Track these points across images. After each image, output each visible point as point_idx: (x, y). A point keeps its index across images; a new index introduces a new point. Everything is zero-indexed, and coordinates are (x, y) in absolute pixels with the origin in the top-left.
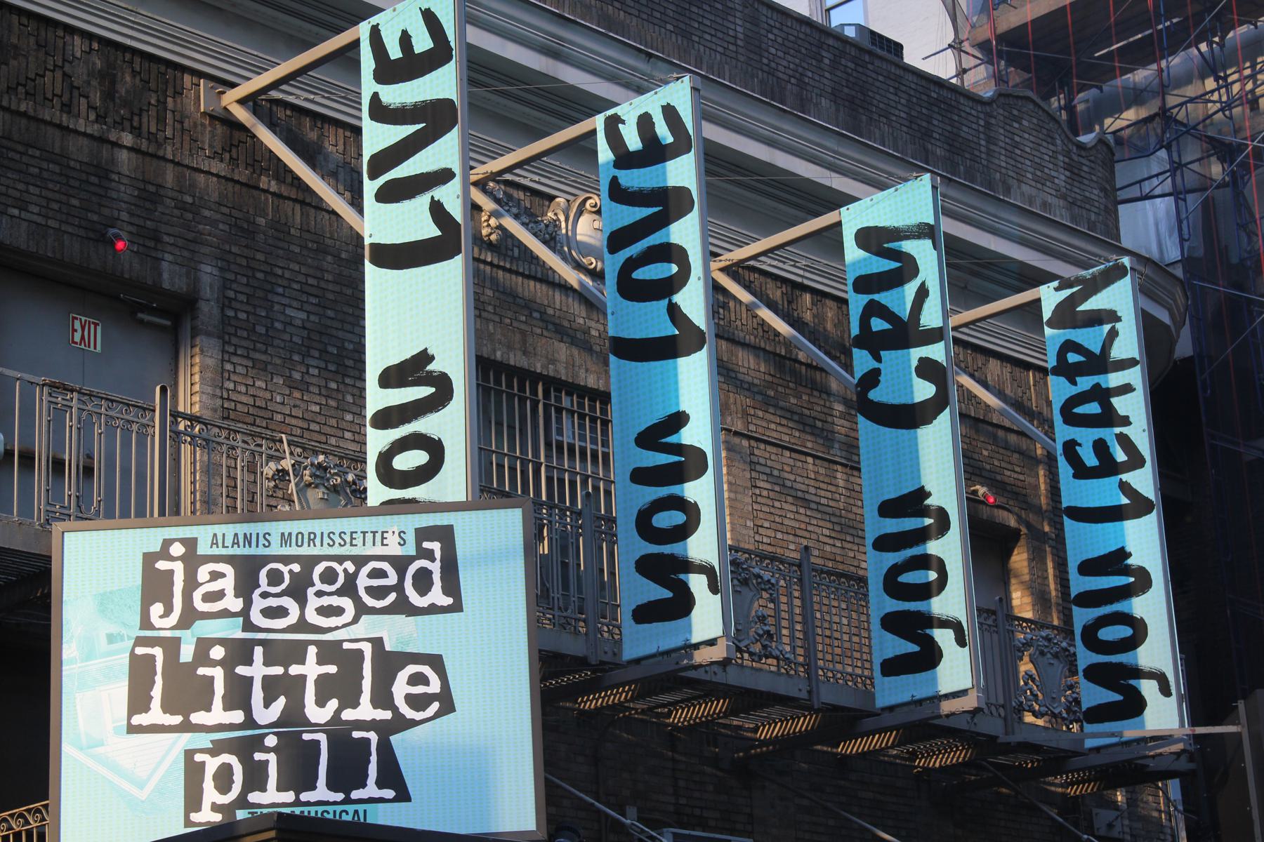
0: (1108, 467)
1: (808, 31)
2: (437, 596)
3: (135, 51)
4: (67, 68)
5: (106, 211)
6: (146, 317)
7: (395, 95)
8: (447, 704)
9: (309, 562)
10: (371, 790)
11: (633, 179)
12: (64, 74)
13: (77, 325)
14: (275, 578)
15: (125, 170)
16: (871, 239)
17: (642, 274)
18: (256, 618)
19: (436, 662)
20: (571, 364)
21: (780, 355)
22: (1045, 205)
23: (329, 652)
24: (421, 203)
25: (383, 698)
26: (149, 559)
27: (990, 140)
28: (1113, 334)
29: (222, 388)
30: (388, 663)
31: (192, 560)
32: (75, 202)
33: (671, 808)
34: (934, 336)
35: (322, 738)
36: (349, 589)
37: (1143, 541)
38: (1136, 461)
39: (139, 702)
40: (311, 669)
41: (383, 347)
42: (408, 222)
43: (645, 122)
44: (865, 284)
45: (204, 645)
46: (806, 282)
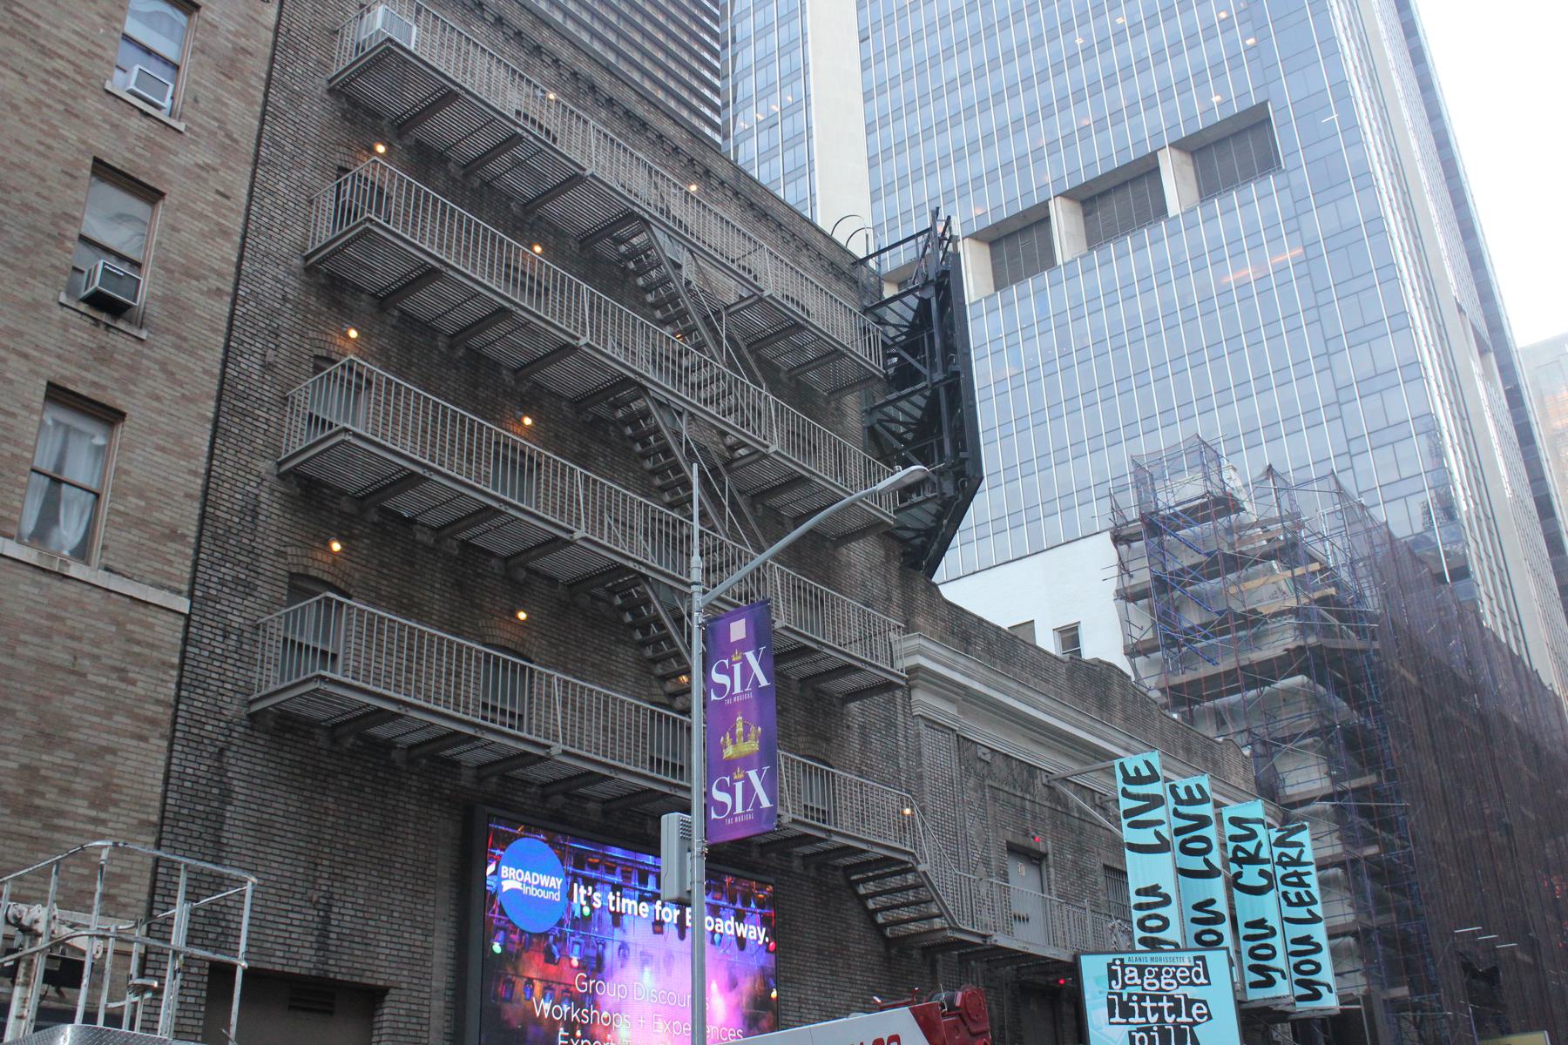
0: (1301, 903)
2: (1202, 980)
7: (1132, 789)
8: (1210, 1018)
9: (1160, 967)
11: (1183, 809)
14: (1150, 973)
16: (1236, 821)
17: (1190, 845)
19: (1205, 1002)
23: (1170, 998)
24: (1151, 830)
25: (1189, 1015)
26: (1109, 965)
28: (1301, 852)
30: (1190, 1003)
31: (1123, 966)
34: (1266, 861)
36: (1174, 977)
38: (1313, 901)
39: (1111, 1015)
40: (1165, 1004)
41: (1135, 881)
42: (1146, 837)
43: (1188, 790)
44: (1233, 838)
45: (1130, 995)
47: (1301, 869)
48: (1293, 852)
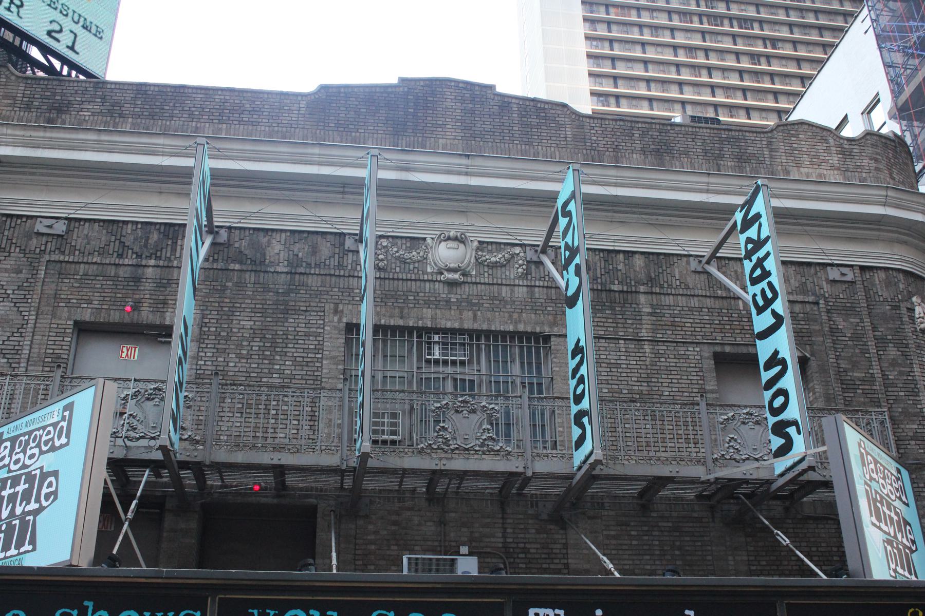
1: (622, 123)
3: (161, 224)
4: (123, 239)
5: (137, 296)
6: (163, 340)
10: (27, 547)
12: (121, 242)
13: (125, 350)
15: (149, 276)
18: (13, 467)
19: (55, 474)
20: (433, 318)
21: (597, 290)
22: (820, 175)
27: (771, 150)
28: (760, 225)
29: (197, 364)
32: (120, 295)
33: (500, 545)
35: (17, 522)
37: (782, 342)
46: (617, 248)
47: (761, 253)
48: (752, 233)
